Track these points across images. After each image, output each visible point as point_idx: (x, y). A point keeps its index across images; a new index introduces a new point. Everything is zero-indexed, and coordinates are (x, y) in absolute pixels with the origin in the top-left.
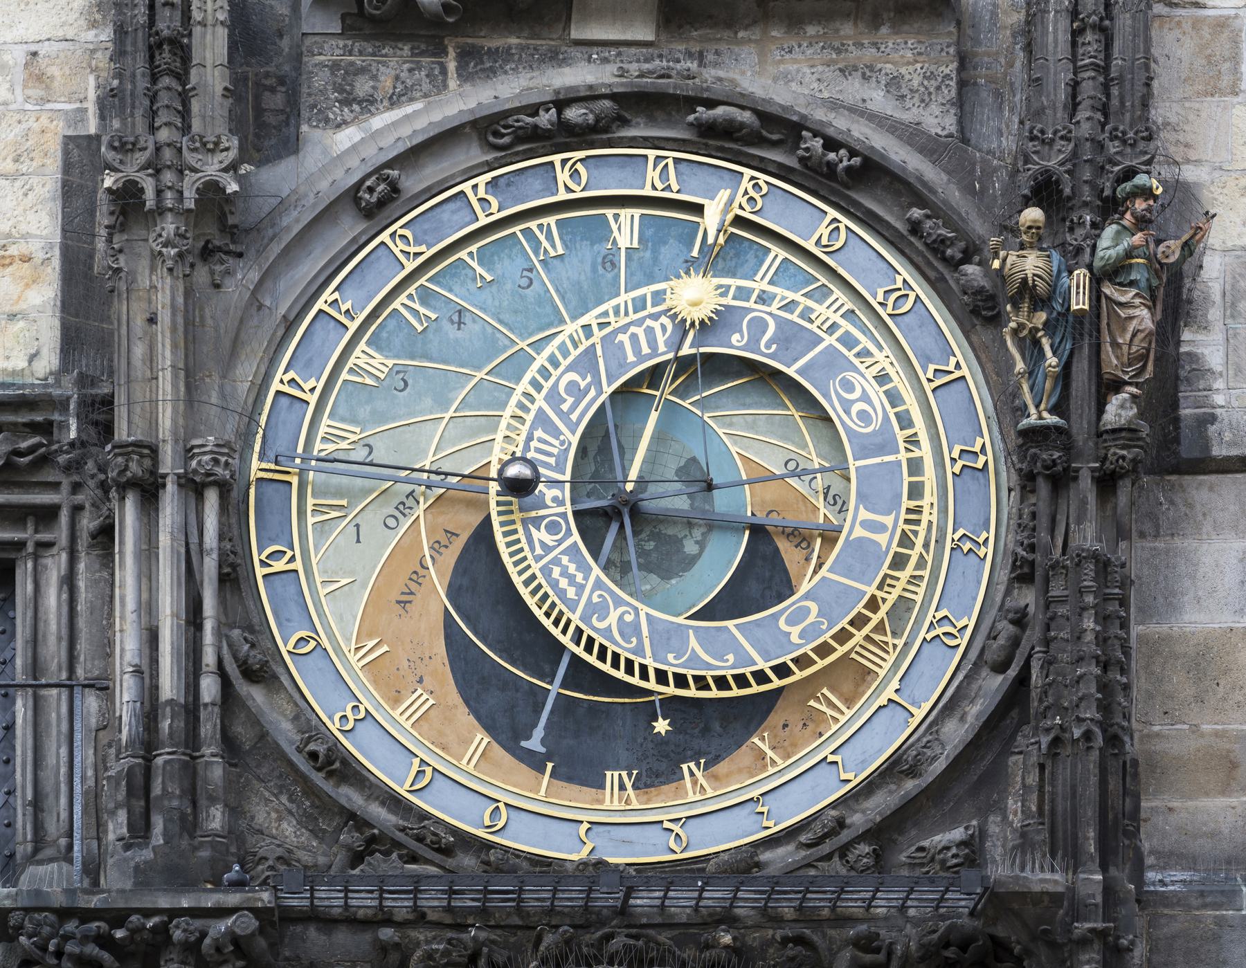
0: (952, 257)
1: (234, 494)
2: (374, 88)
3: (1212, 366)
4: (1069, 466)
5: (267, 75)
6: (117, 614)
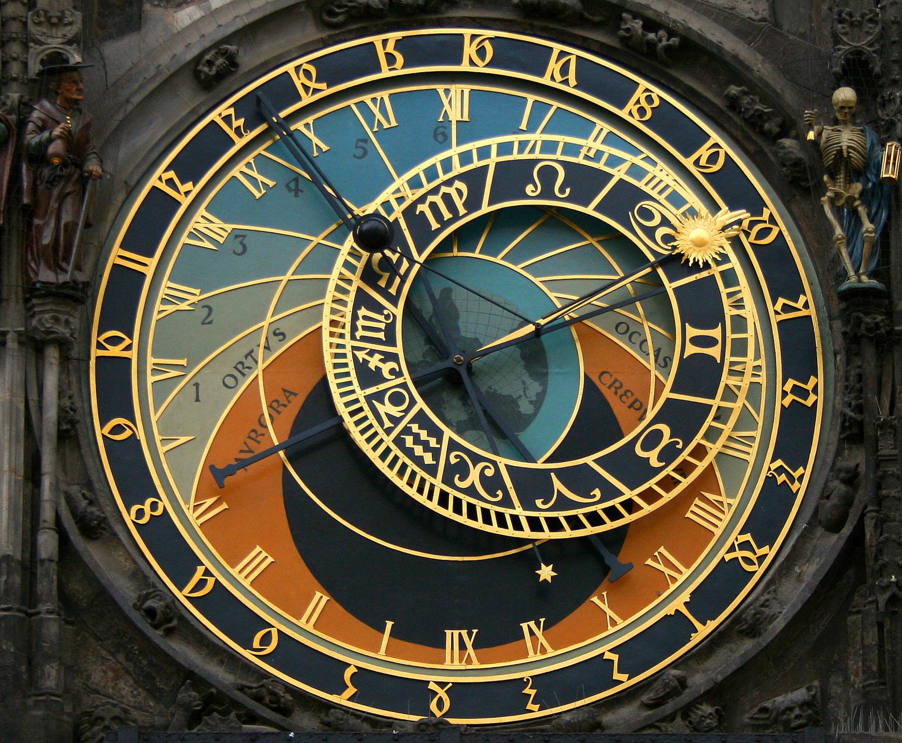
0: (770, 131)
1: (74, 353)
4: (892, 330)
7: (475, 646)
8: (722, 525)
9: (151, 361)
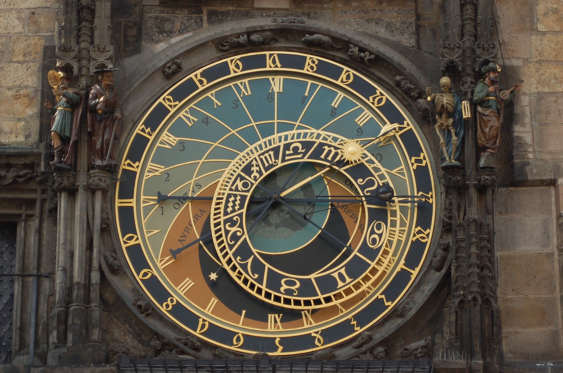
0: (414, 96)
2: (173, 27)
3: (527, 141)
5: (129, 22)
6: (57, 245)
9: (142, 197)
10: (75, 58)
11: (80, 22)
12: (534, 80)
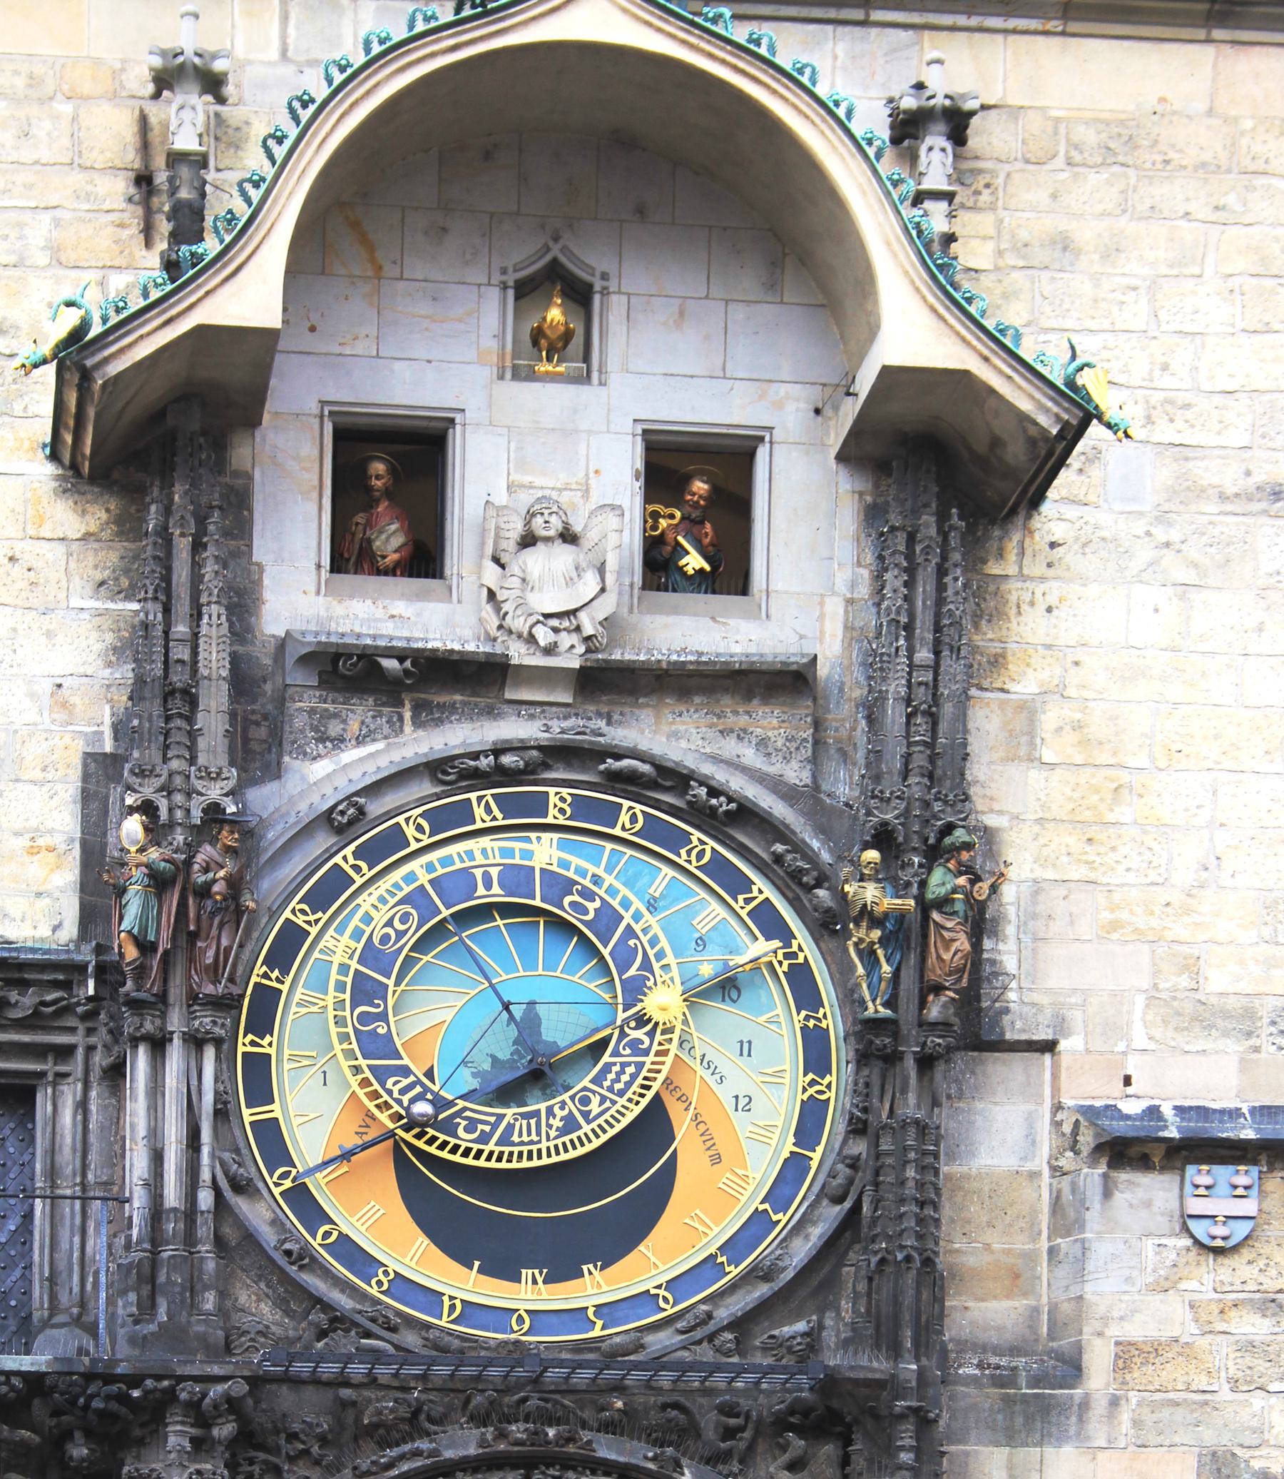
0: (807, 883)
7: (545, 1282)
8: (747, 1194)
10: (161, 789)
11: (168, 719)
12: (1028, 856)
